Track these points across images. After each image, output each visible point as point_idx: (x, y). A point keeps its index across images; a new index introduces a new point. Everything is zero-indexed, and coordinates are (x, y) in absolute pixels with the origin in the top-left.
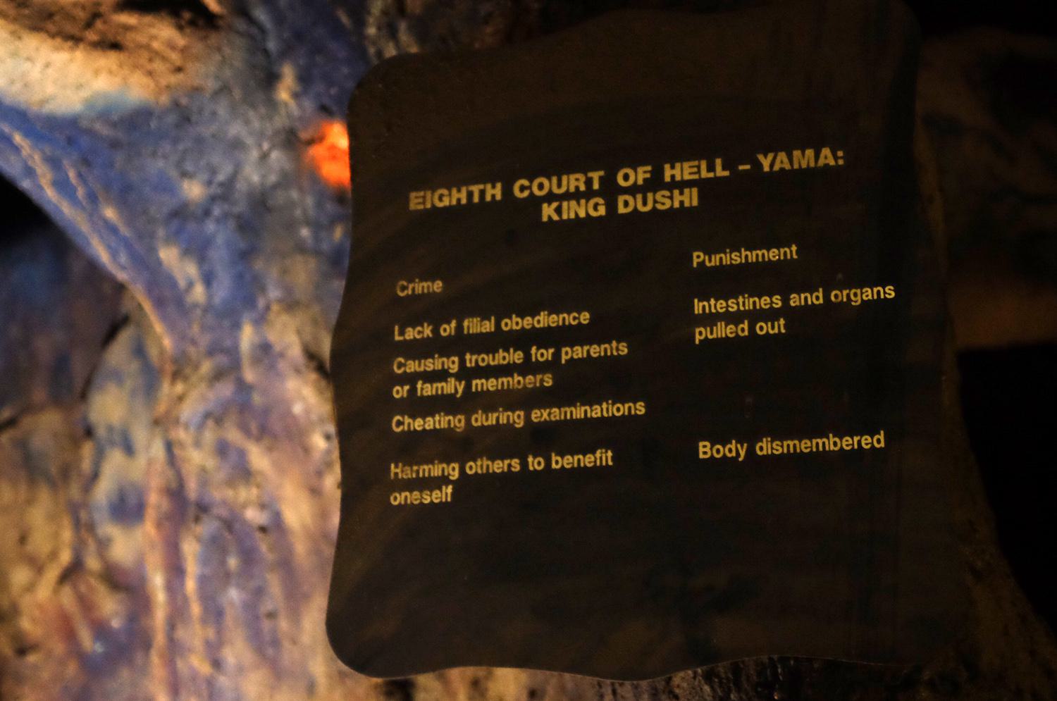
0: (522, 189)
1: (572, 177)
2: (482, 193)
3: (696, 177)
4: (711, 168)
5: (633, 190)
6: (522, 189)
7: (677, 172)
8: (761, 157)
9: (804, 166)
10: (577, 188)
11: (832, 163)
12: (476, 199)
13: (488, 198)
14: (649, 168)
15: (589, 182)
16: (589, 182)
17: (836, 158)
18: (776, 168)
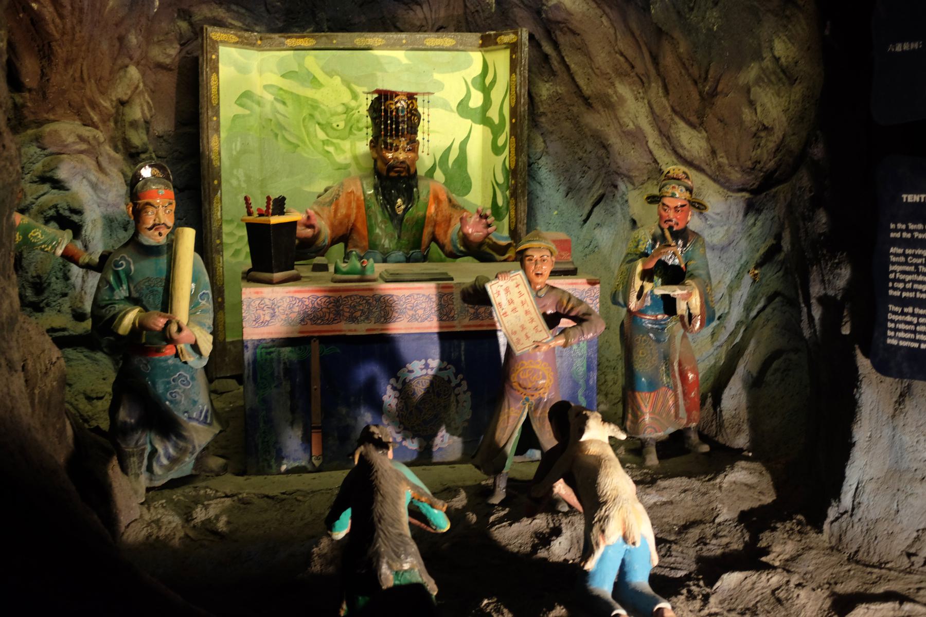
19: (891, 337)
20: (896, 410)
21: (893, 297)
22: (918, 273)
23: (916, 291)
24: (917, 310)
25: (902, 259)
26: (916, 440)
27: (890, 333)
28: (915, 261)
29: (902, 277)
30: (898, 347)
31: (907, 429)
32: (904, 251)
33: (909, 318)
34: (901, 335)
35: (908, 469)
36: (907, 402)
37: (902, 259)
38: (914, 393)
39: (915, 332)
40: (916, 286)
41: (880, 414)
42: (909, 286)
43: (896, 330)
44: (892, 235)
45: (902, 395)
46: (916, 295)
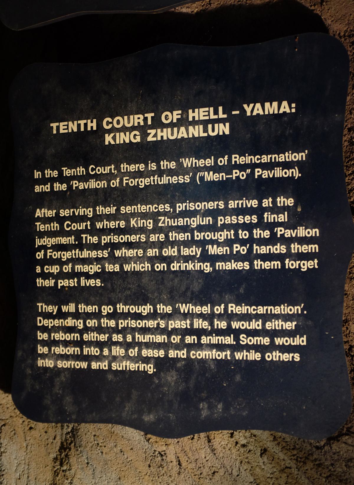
0: (108, 123)
1: (136, 116)
2: (86, 125)
3: (207, 118)
4: (216, 112)
5: (172, 125)
6: (108, 123)
7: (196, 114)
8: (245, 106)
9: (271, 112)
10: (139, 123)
11: (288, 111)
12: (82, 129)
13: (89, 129)
14: (180, 112)
15: (146, 119)
16: (146, 119)
17: (291, 108)
18: (255, 114)
19: (43, 356)
21: (43, 288)
22: (81, 246)
23: (79, 275)
24: (82, 307)
25: (55, 226)
27: (42, 350)
28: (75, 226)
29: (56, 255)
30: (56, 372)
32: (57, 214)
33: (70, 322)
34: (59, 350)
36: (73, 460)
37: (55, 226)
38: (83, 443)
39: (80, 344)
40: (79, 268)
42: (67, 268)
44: (38, 189)
46: (79, 282)
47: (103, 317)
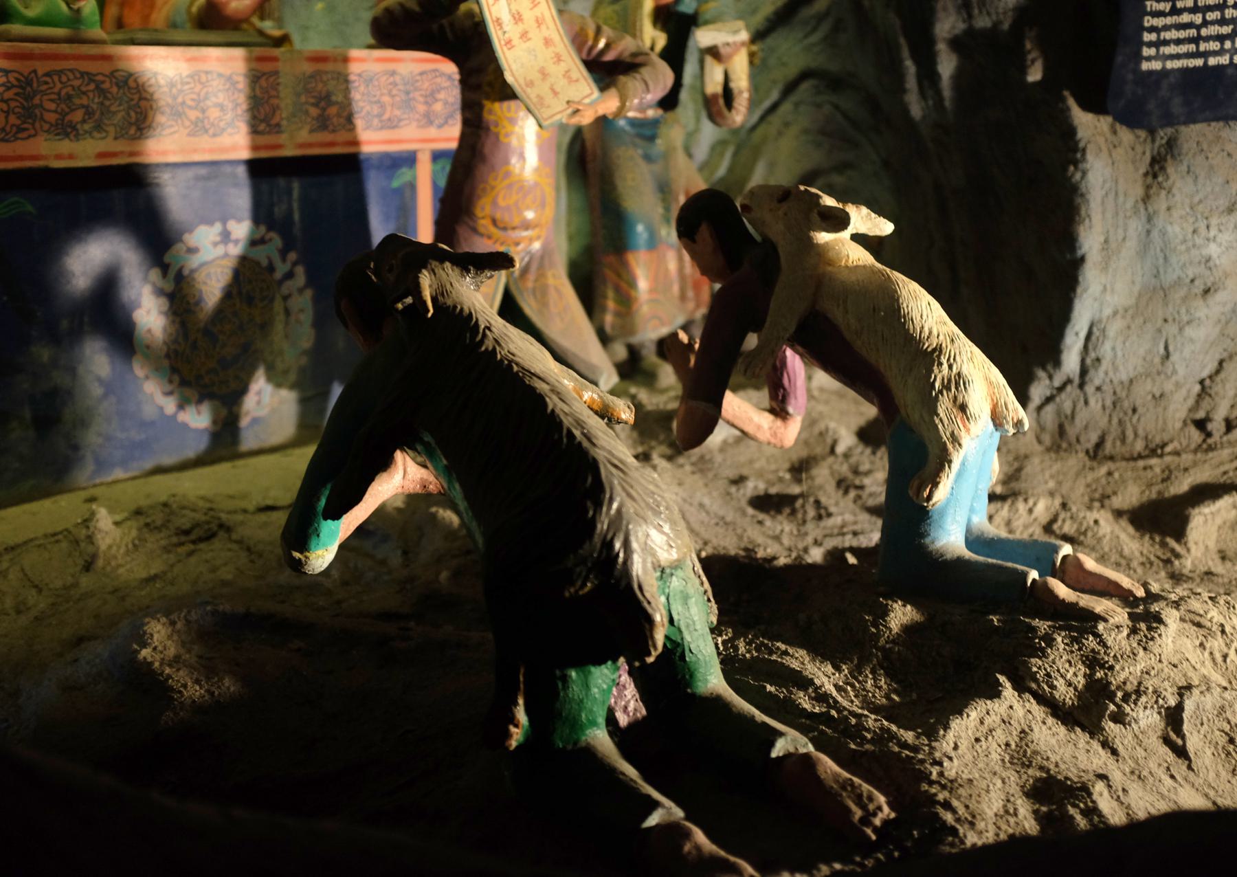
19: (1149, 59)
20: (1148, 187)
26: (1191, 230)
30: (1164, 73)
31: (1176, 214)
35: (1178, 283)
39: (1196, 40)
41: (1121, 199)
43: (1158, 44)
45: (1154, 161)
47: (1228, 7)
